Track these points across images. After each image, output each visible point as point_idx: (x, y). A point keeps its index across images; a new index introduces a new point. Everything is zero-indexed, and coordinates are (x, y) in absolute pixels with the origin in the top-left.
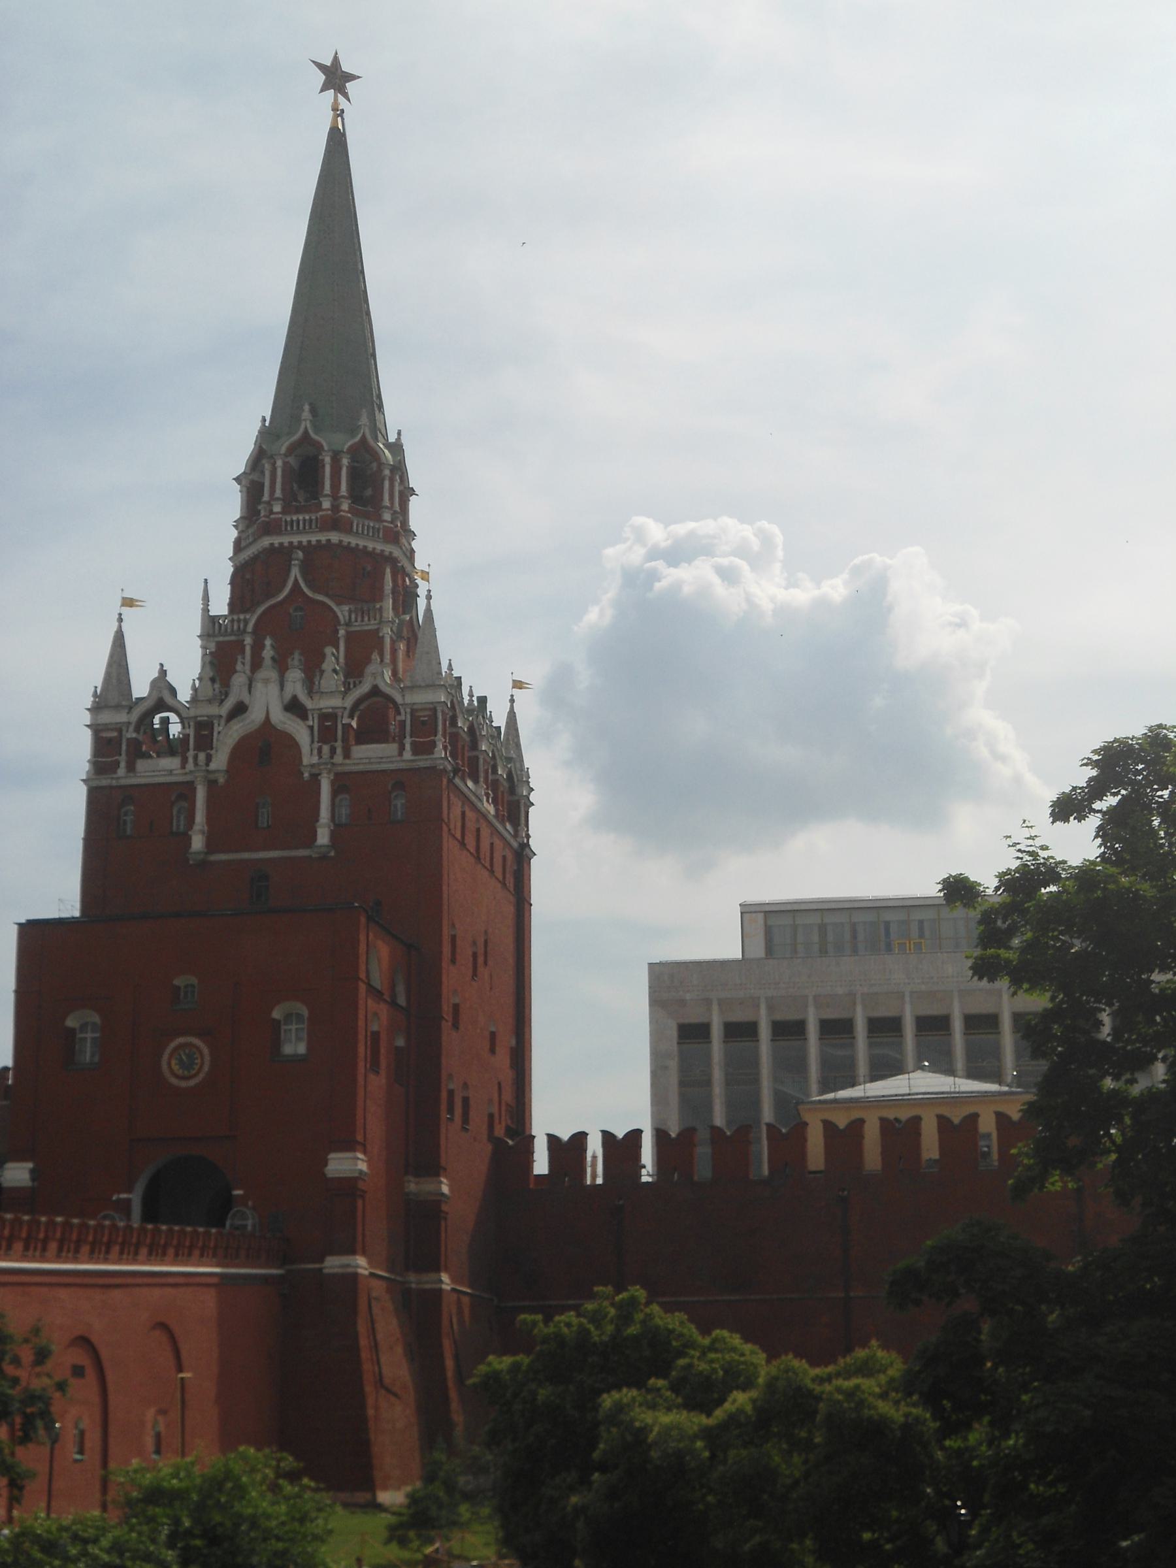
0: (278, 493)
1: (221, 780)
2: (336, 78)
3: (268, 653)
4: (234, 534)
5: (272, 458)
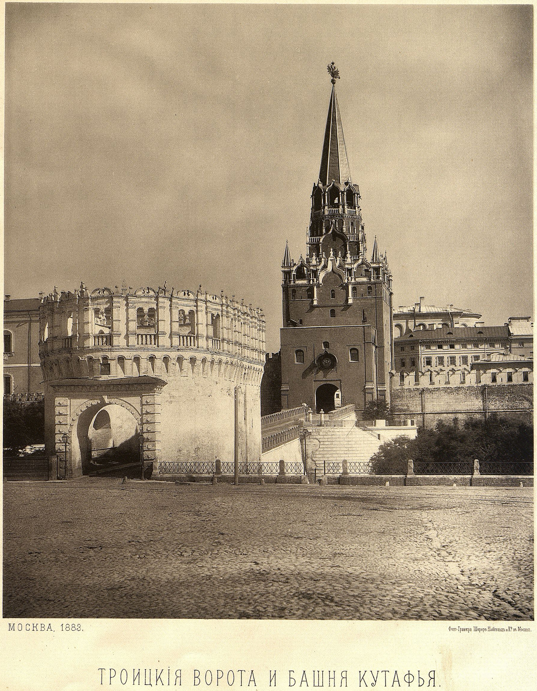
3: (332, 253)
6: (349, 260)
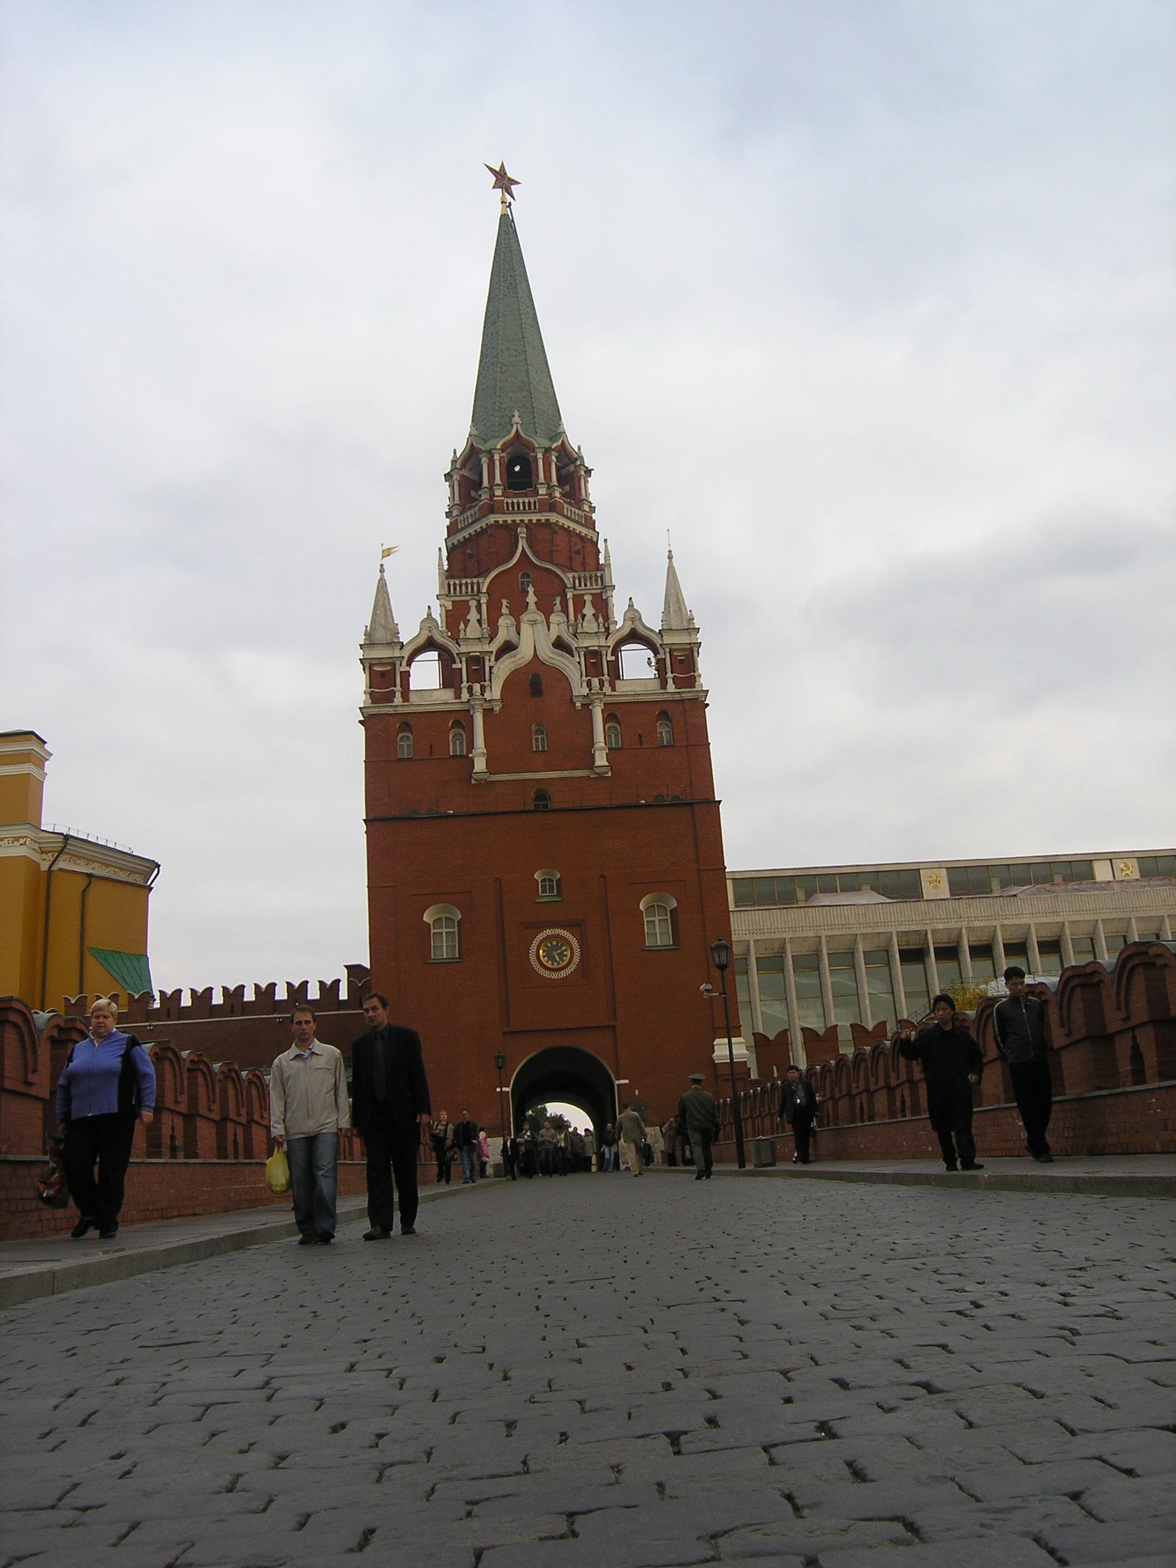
0: (498, 480)
1: (497, 709)
2: (503, 181)
3: (531, 599)
4: (448, 521)
5: (490, 453)
6: (590, 625)
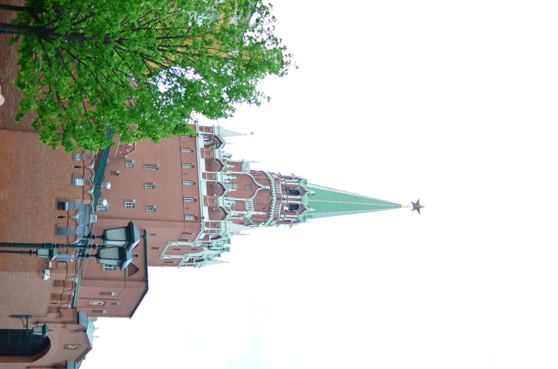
5: (300, 200)
